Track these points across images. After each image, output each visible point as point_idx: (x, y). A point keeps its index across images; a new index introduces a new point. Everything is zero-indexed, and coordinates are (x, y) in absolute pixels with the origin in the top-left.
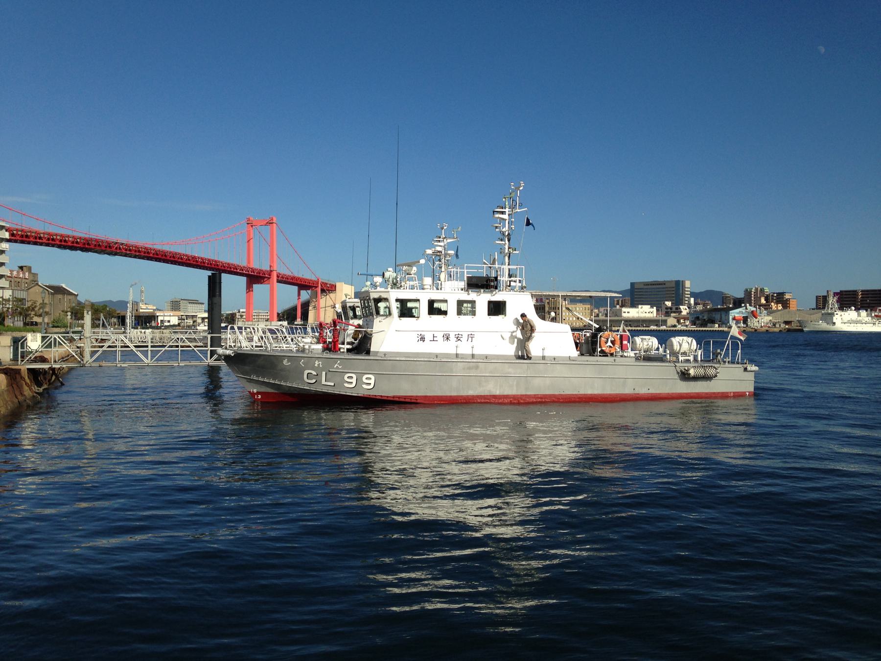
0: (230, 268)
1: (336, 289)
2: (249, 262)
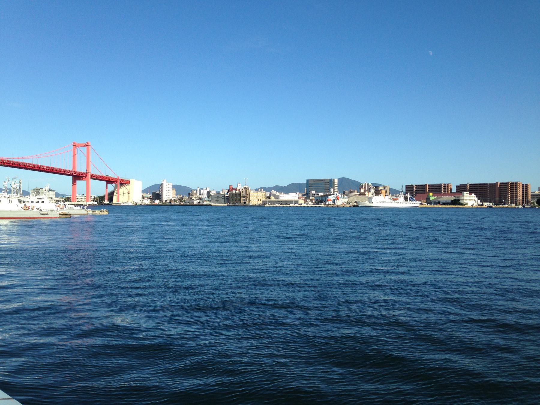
0: (61, 171)
2: (74, 166)
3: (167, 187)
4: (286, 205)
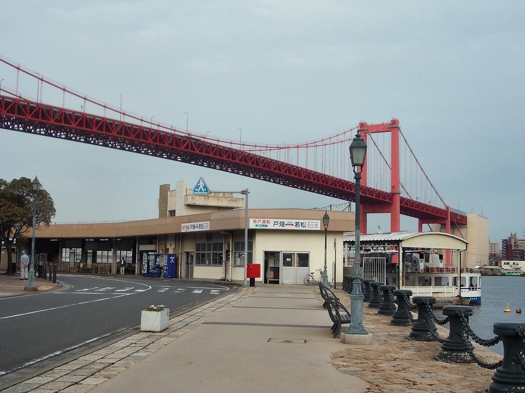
1: (466, 223)
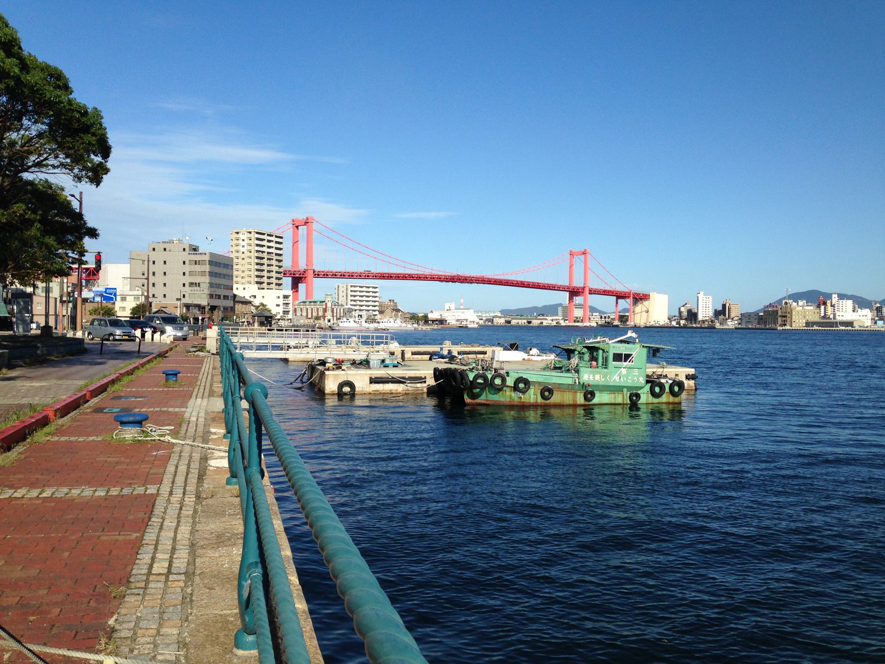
3: (704, 301)
4: (834, 329)
